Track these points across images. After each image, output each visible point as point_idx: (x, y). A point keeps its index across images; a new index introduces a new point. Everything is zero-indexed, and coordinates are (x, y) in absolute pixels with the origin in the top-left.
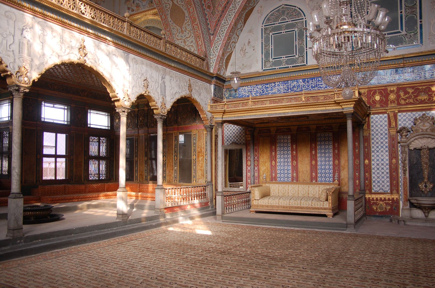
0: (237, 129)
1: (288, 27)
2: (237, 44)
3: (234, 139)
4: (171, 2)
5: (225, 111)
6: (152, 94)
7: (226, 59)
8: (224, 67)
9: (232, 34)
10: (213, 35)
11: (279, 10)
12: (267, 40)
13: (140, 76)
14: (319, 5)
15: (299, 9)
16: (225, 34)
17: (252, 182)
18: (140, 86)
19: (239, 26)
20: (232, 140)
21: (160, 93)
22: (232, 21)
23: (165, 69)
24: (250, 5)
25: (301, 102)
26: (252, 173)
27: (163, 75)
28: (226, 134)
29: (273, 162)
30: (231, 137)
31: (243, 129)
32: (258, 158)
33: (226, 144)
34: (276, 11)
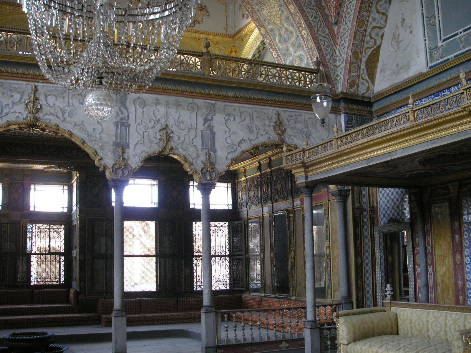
0: (397, 193)
2: (387, 30)
3: (393, 211)
5: (302, 163)
6: (181, 150)
7: (368, 62)
8: (367, 78)
9: (364, 13)
10: (336, 23)
13: (151, 125)
16: (352, 16)
17: (424, 299)
18: (151, 142)
20: (391, 216)
21: (199, 146)
23: (212, 104)
25: (408, 124)
26: (424, 279)
27: (208, 114)
28: (381, 203)
29: (458, 256)
30: (388, 208)
31: (406, 192)
32: (432, 247)
33: (382, 223)
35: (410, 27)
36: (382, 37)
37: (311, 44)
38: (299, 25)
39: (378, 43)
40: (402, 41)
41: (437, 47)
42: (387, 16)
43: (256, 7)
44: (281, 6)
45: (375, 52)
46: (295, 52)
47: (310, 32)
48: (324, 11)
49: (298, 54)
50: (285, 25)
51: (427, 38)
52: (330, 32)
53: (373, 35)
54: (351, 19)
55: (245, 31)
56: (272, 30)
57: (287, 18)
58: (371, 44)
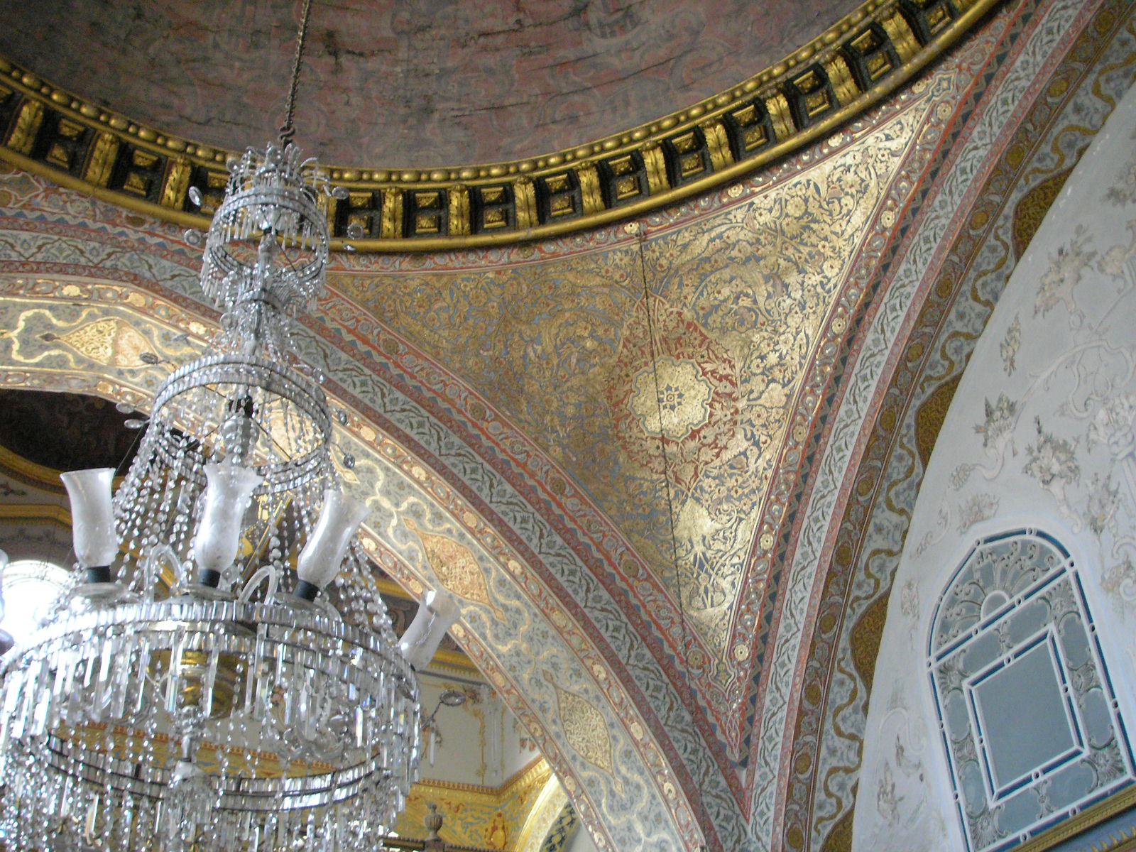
1: (1018, 629)
4: (550, 686)
9: (809, 738)
10: (744, 763)
11: (970, 571)
12: (958, 718)
14: (1106, 486)
15: (1041, 534)
16: (779, 746)
19: (839, 695)
22: (794, 685)
24: (856, 592)
34: (963, 582)
35: (919, 765)
36: (854, 790)
37: (687, 815)
38: (655, 770)
39: (846, 805)
40: (901, 799)
41: (985, 811)
42: (861, 743)
43: (553, 729)
44: (612, 725)
45: (840, 828)
46: (649, 835)
47: (683, 785)
48: (713, 734)
49: (654, 838)
50: (623, 770)
51: (959, 791)
52: (730, 785)
53: (833, 788)
54: (778, 751)
55: (527, 780)
56: (591, 782)
57: (628, 754)
58: (830, 809)
